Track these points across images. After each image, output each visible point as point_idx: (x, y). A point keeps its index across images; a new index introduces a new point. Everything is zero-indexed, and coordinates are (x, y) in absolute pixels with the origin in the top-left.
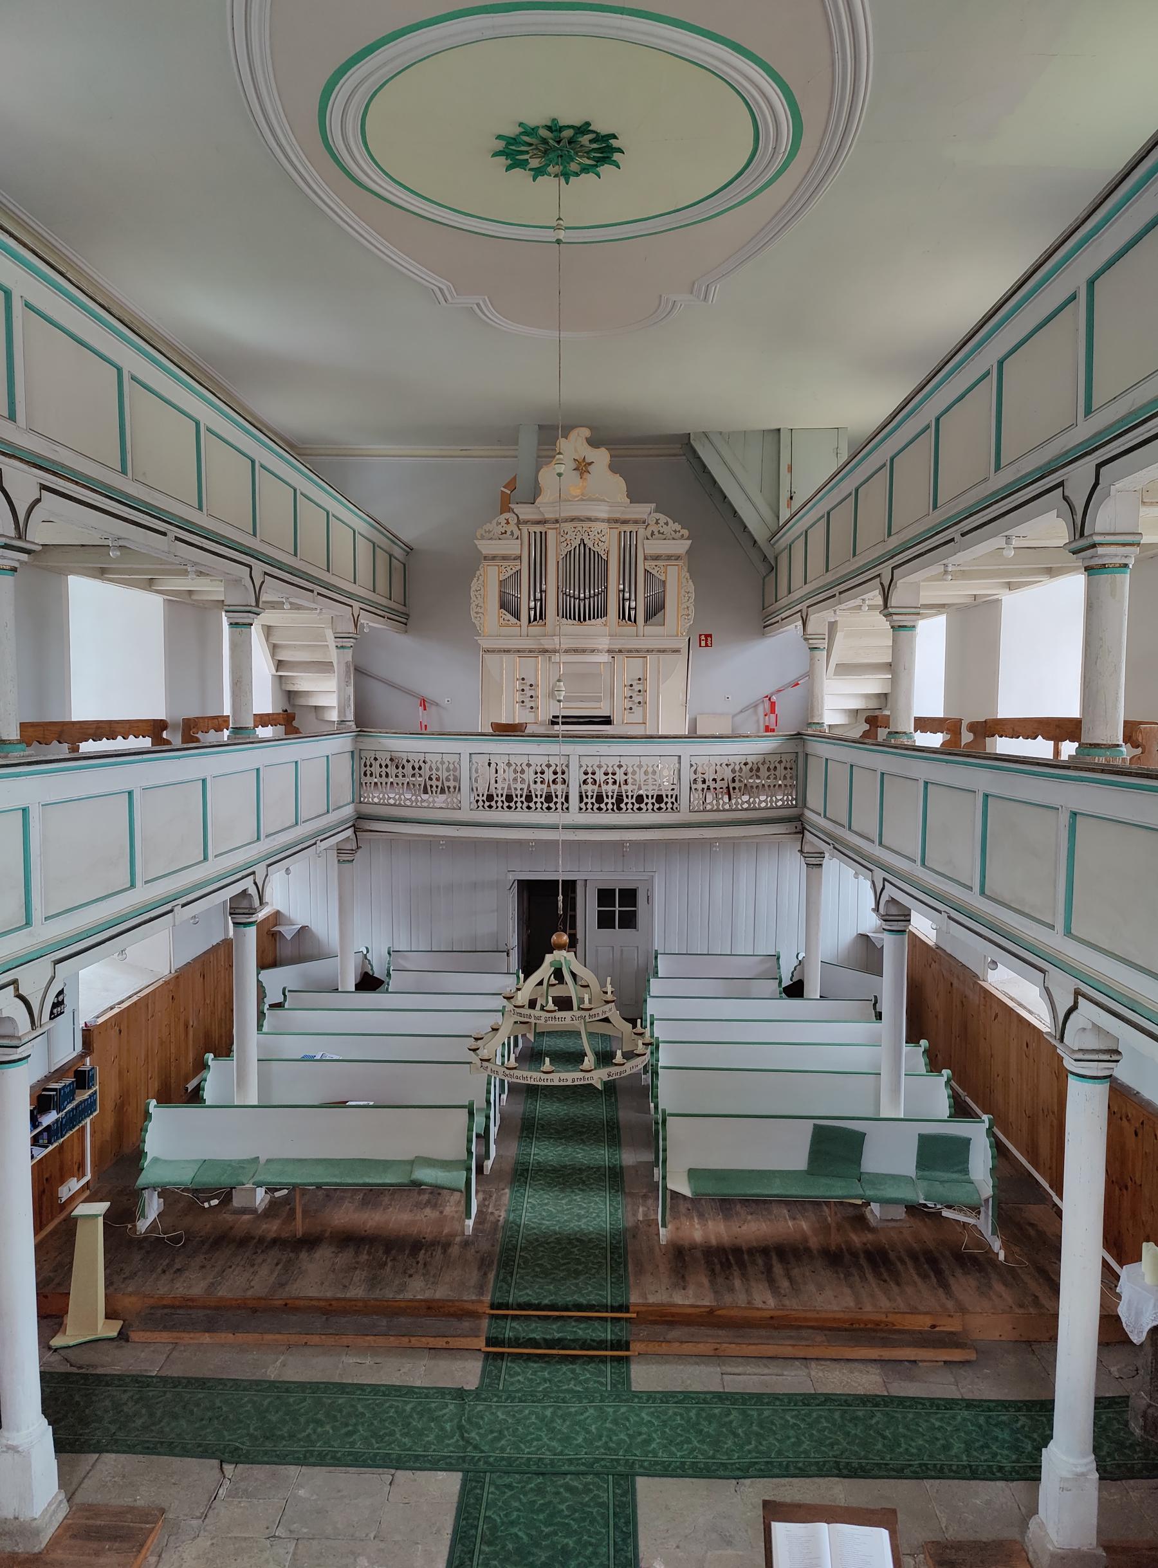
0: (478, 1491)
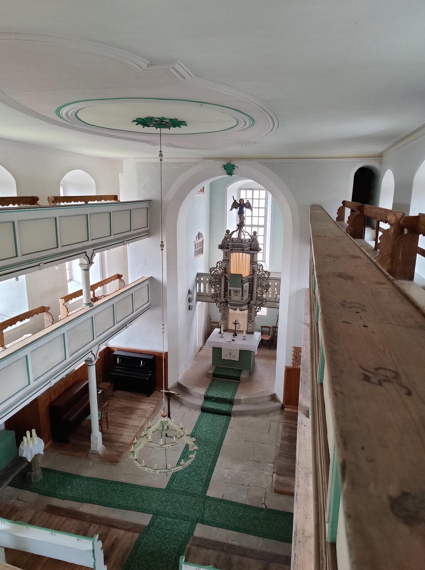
0: (203, 490)
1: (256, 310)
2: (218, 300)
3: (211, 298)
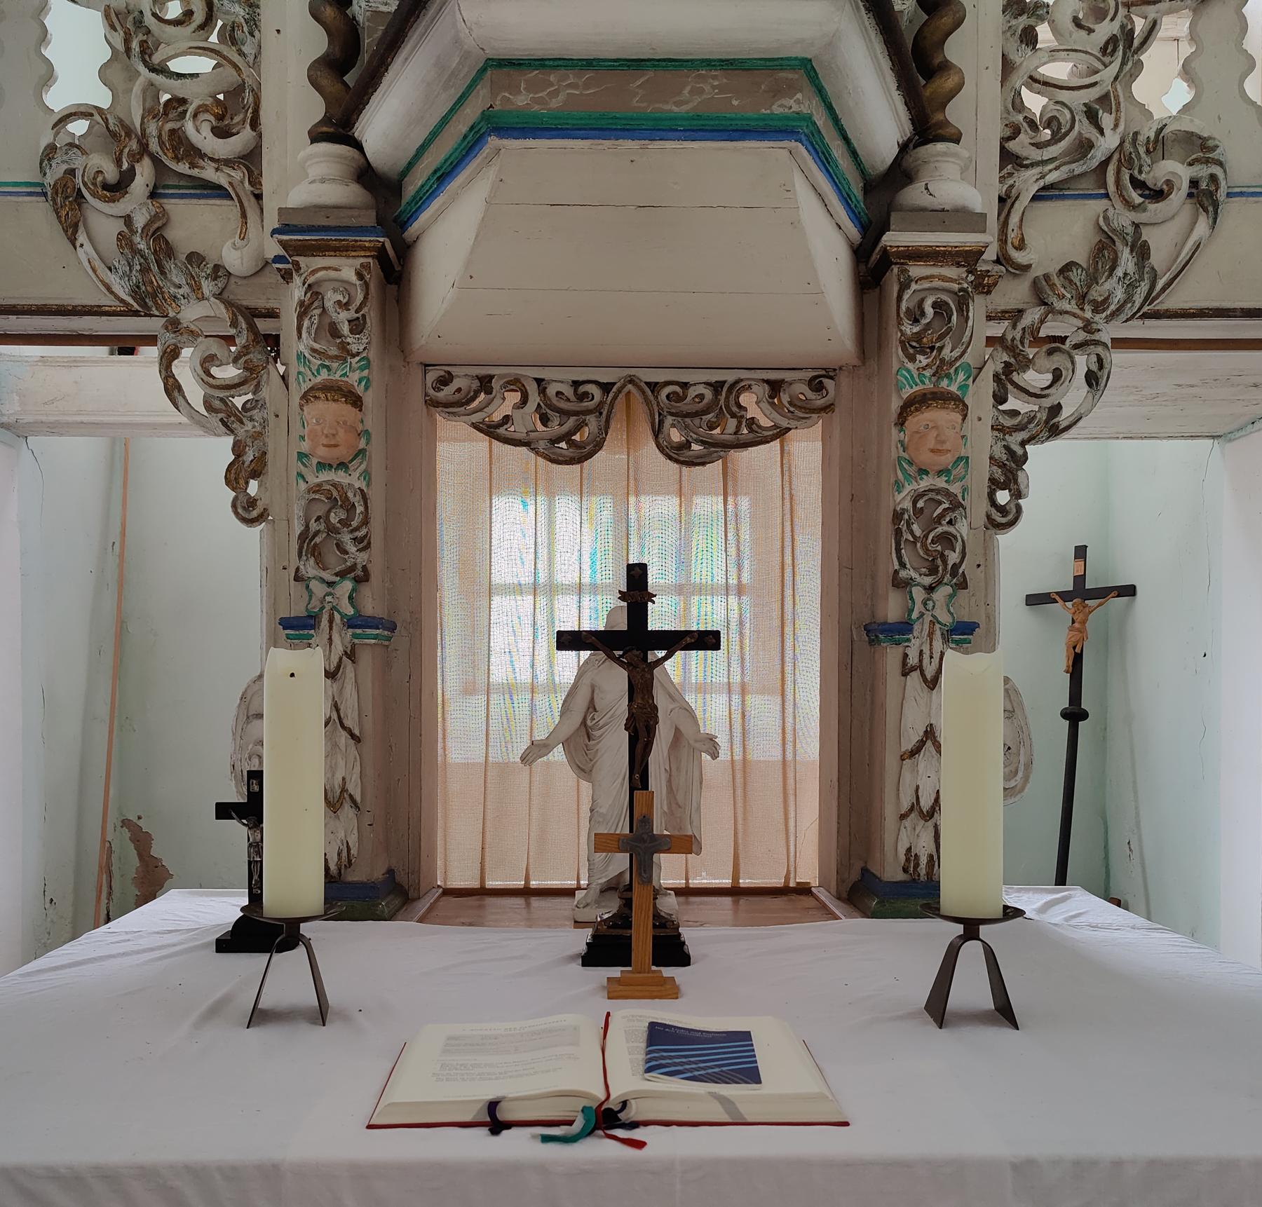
1: (1012, 403)
2: (195, 258)
3: (39, 214)
